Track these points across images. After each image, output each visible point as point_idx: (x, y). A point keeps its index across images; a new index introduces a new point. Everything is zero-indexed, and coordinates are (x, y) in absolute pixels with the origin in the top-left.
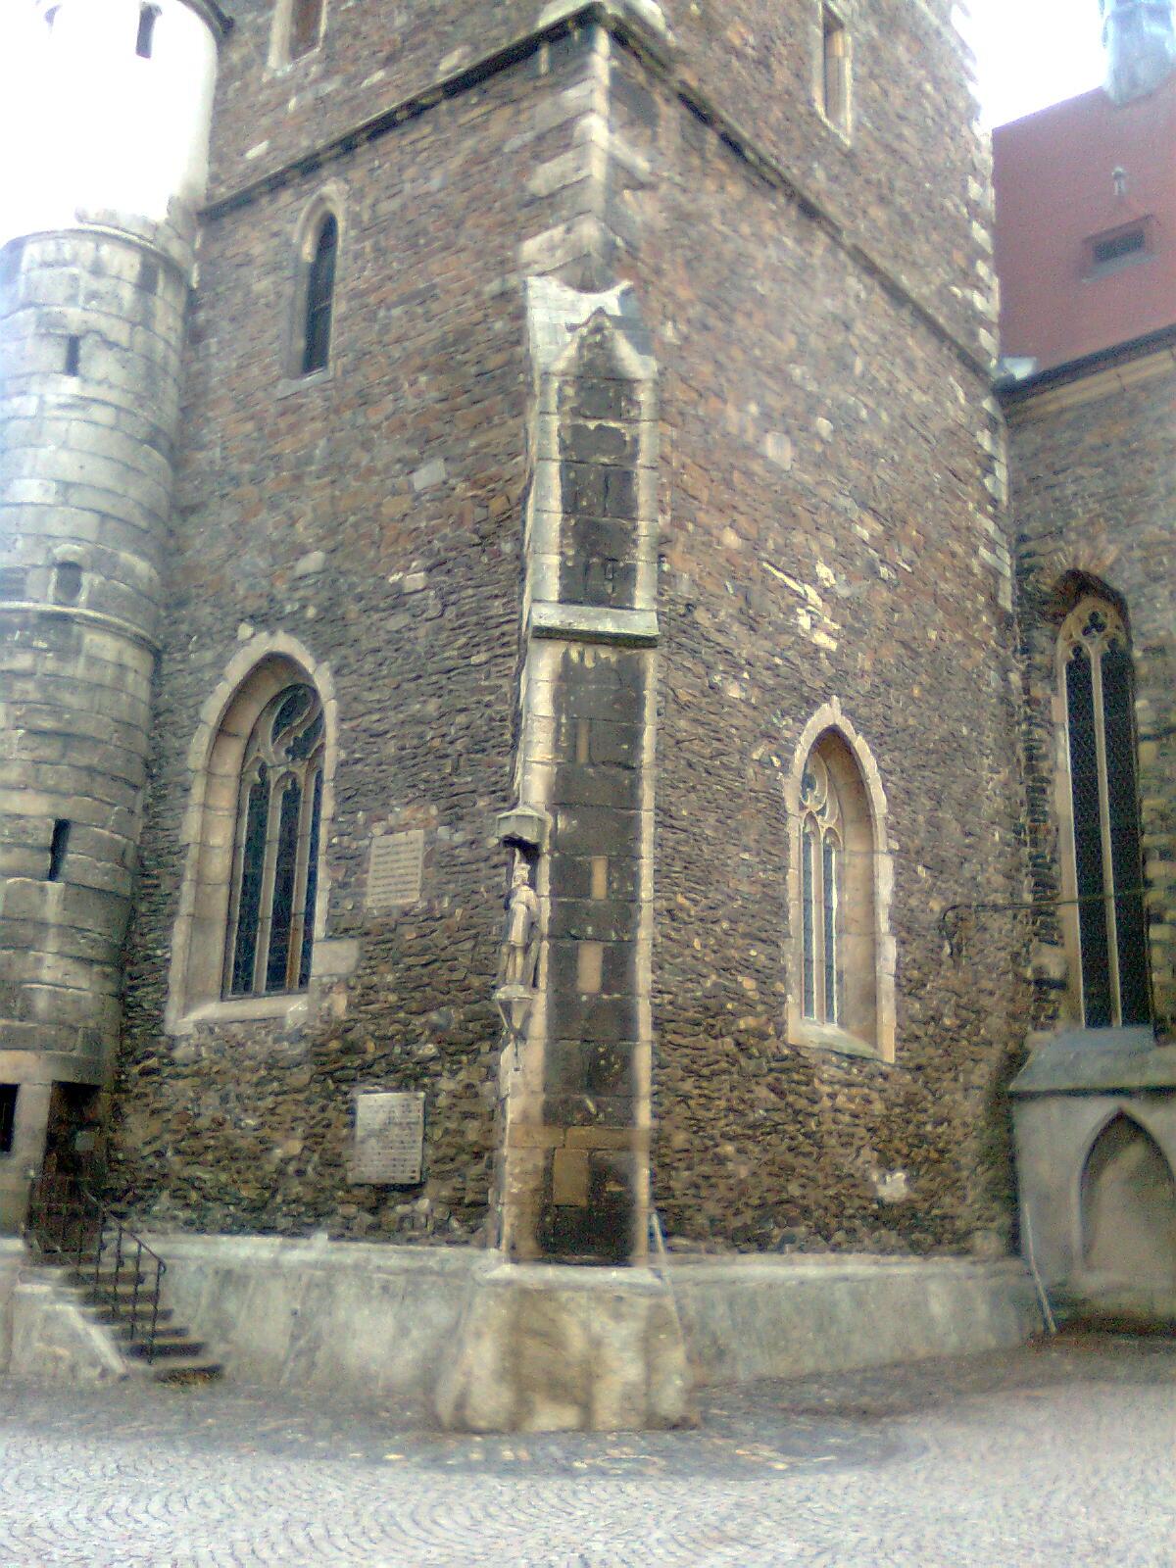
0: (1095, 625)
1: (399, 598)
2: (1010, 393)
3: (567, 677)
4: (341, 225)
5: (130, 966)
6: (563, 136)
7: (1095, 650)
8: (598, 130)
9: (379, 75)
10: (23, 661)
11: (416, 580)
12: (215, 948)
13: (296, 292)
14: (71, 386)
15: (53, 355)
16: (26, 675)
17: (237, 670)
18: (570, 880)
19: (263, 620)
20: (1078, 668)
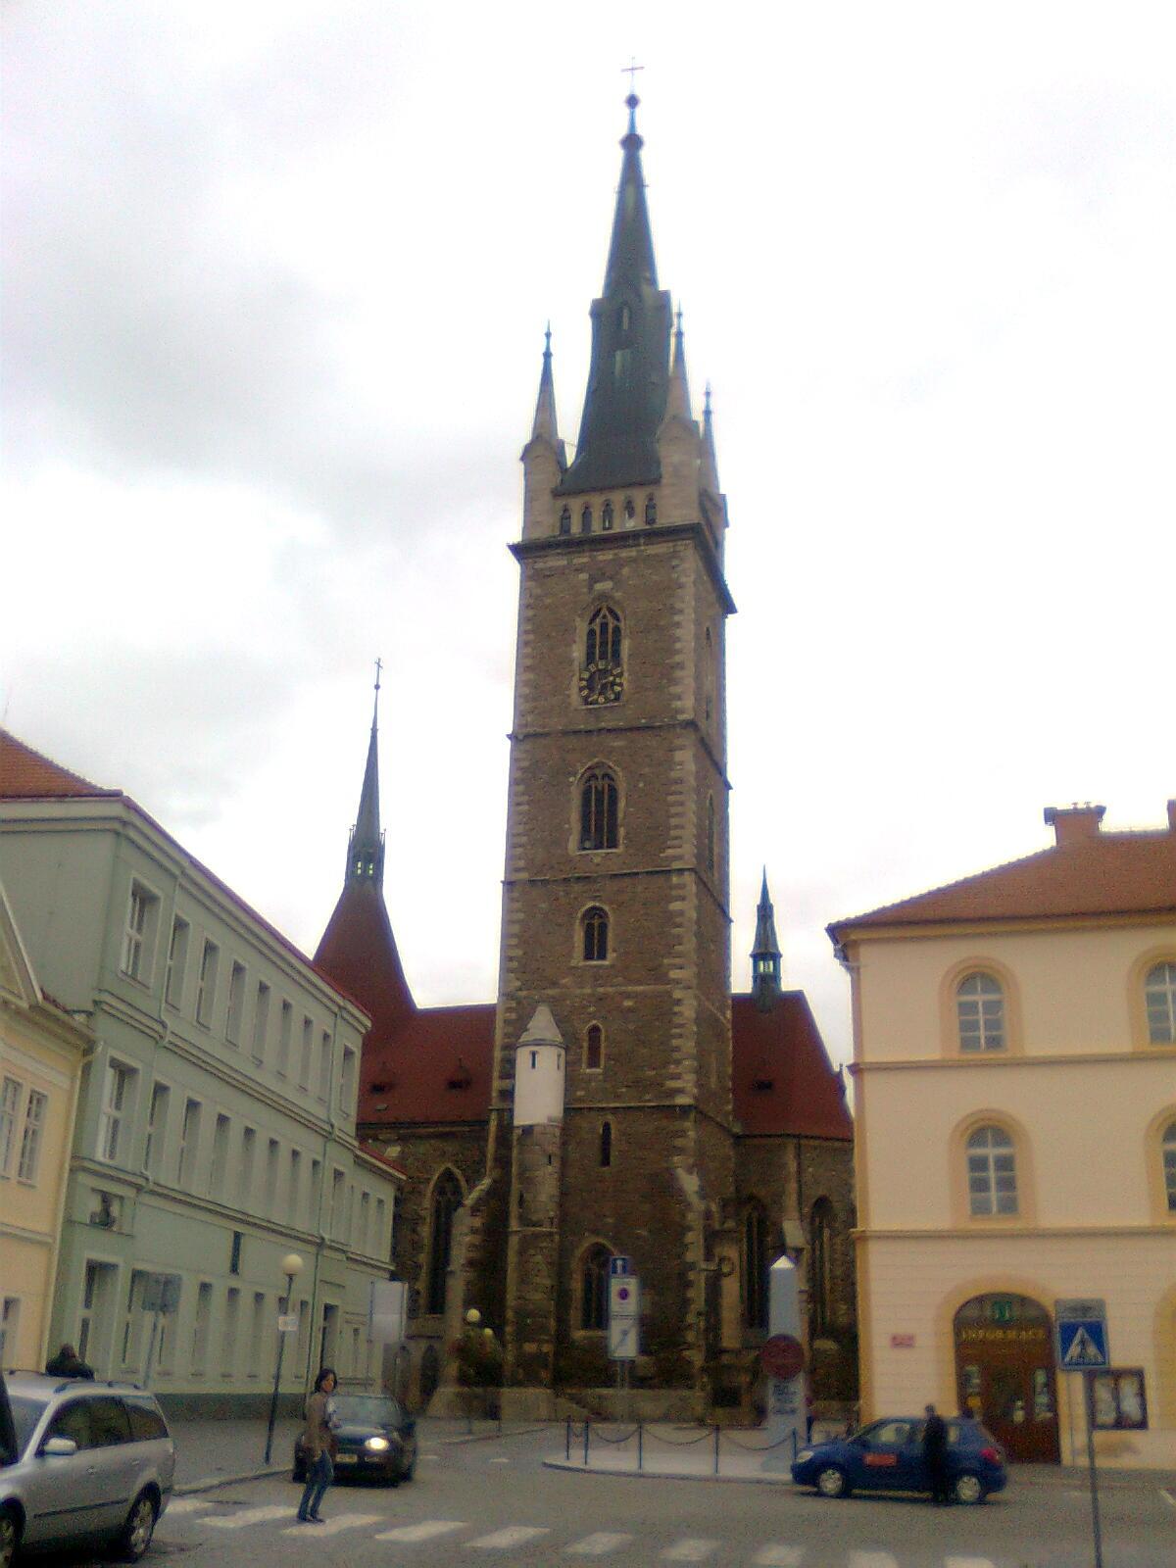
0: (755, 1208)
1: (639, 1237)
2: (737, 1137)
3: (707, 1279)
4: (612, 1126)
5: (562, 1320)
6: (682, 1134)
7: (755, 1215)
8: (691, 1134)
9: (624, 1090)
10: (545, 1244)
11: (644, 1233)
12: (579, 1315)
13: (598, 1142)
14: (550, 1169)
15: (546, 1160)
16: (546, 1248)
17: (586, 1245)
18: (707, 1321)
19: (595, 1232)
20: (749, 1218)
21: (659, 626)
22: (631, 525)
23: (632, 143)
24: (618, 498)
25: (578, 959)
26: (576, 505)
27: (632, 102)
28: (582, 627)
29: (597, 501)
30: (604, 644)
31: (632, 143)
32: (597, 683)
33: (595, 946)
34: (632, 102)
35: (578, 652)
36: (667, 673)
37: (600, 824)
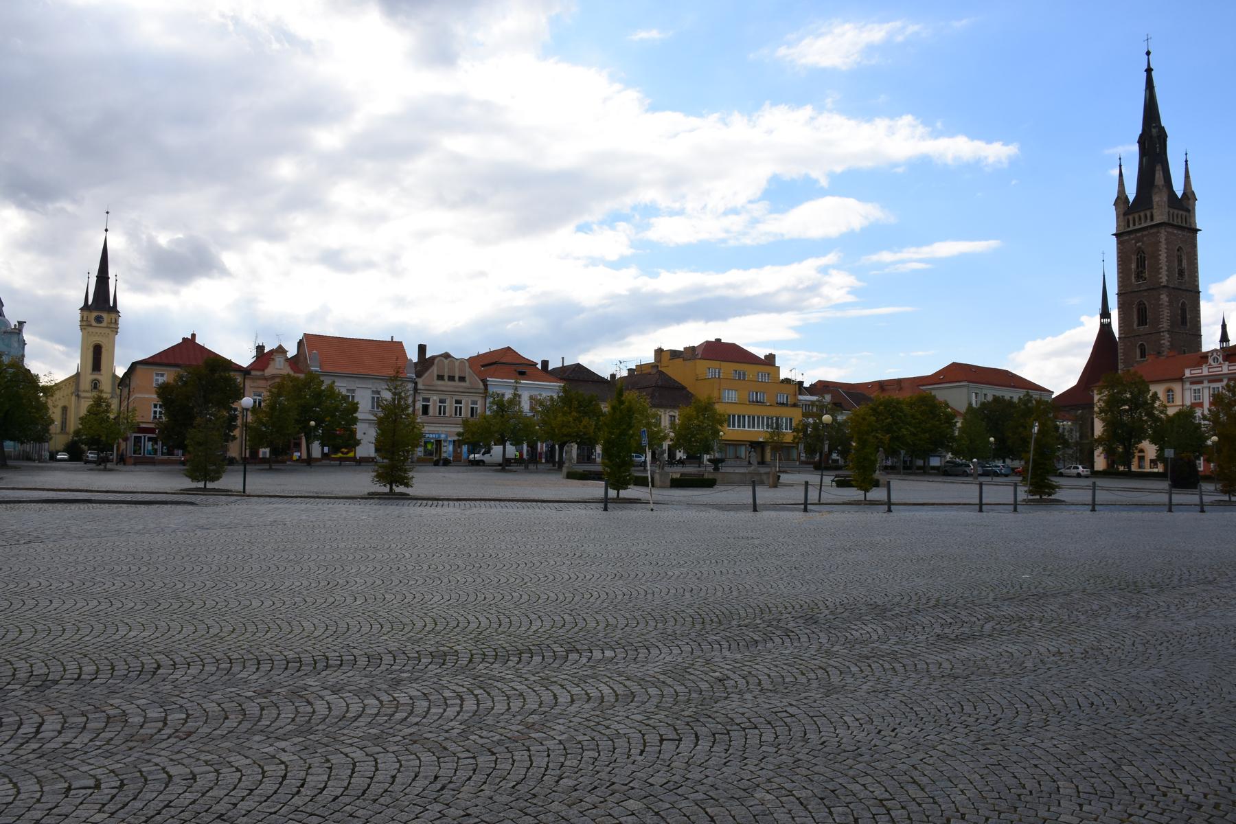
21: (1156, 257)
22: (1149, 223)
23: (1149, 71)
24: (1142, 214)
25: (1138, 359)
26: (1131, 218)
27: (1148, 53)
28: (1134, 257)
29: (1136, 216)
30: (1141, 263)
31: (1149, 71)
32: (1139, 276)
33: (1143, 355)
34: (1148, 53)
35: (1133, 266)
36: (1158, 271)
37: (1142, 321)
